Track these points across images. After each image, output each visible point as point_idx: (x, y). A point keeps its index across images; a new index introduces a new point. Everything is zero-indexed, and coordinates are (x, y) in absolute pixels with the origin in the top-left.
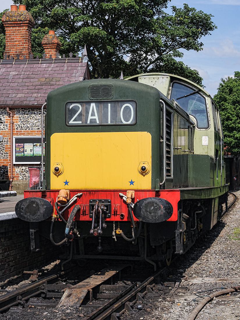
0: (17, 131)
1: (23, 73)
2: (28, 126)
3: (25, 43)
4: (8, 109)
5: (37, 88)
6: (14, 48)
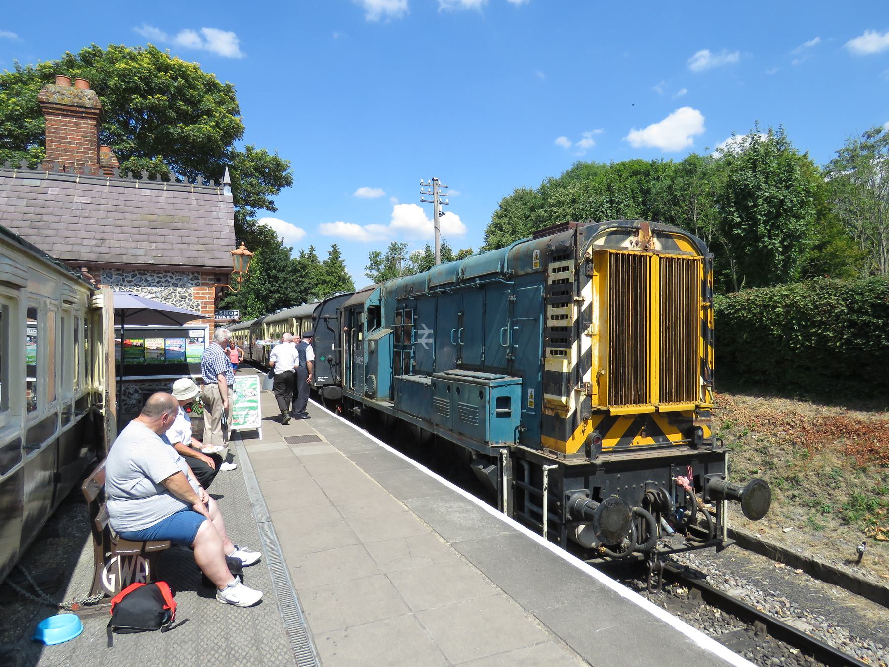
3: (90, 149)
4: (84, 269)
5: (143, 231)
6: (66, 155)
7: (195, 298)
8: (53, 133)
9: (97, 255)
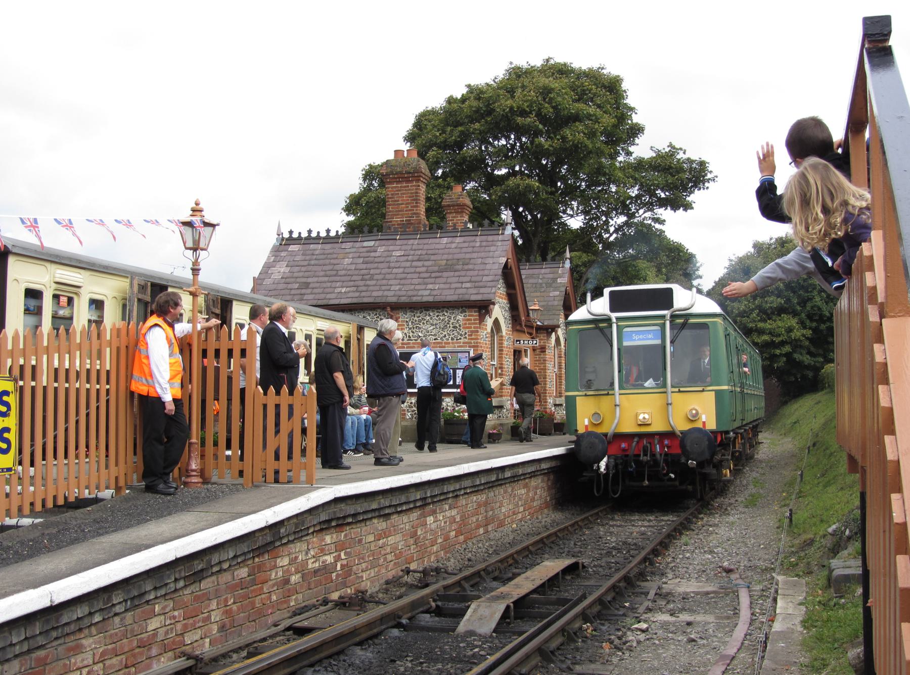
0: (402, 344)
1: (412, 252)
2: (420, 334)
4: (389, 309)
5: (433, 275)
6: (398, 215)
7: (464, 328)
8: (390, 198)
9: (397, 298)
